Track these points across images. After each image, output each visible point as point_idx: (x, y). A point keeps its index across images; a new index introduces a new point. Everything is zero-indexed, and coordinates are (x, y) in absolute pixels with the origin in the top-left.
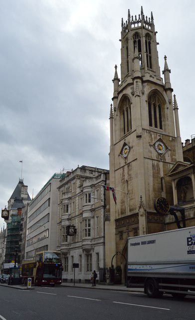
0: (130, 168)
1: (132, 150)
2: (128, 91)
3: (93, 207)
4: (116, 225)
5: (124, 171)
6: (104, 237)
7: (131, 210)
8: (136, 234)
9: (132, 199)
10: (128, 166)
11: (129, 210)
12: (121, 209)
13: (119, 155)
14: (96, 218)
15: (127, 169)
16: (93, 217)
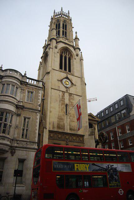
0: (71, 97)
1: (74, 86)
2: (72, 49)
5: (64, 94)
7: (71, 129)
9: (74, 122)
11: (68, 127)
13: (58, 80)
15: (68, 96)
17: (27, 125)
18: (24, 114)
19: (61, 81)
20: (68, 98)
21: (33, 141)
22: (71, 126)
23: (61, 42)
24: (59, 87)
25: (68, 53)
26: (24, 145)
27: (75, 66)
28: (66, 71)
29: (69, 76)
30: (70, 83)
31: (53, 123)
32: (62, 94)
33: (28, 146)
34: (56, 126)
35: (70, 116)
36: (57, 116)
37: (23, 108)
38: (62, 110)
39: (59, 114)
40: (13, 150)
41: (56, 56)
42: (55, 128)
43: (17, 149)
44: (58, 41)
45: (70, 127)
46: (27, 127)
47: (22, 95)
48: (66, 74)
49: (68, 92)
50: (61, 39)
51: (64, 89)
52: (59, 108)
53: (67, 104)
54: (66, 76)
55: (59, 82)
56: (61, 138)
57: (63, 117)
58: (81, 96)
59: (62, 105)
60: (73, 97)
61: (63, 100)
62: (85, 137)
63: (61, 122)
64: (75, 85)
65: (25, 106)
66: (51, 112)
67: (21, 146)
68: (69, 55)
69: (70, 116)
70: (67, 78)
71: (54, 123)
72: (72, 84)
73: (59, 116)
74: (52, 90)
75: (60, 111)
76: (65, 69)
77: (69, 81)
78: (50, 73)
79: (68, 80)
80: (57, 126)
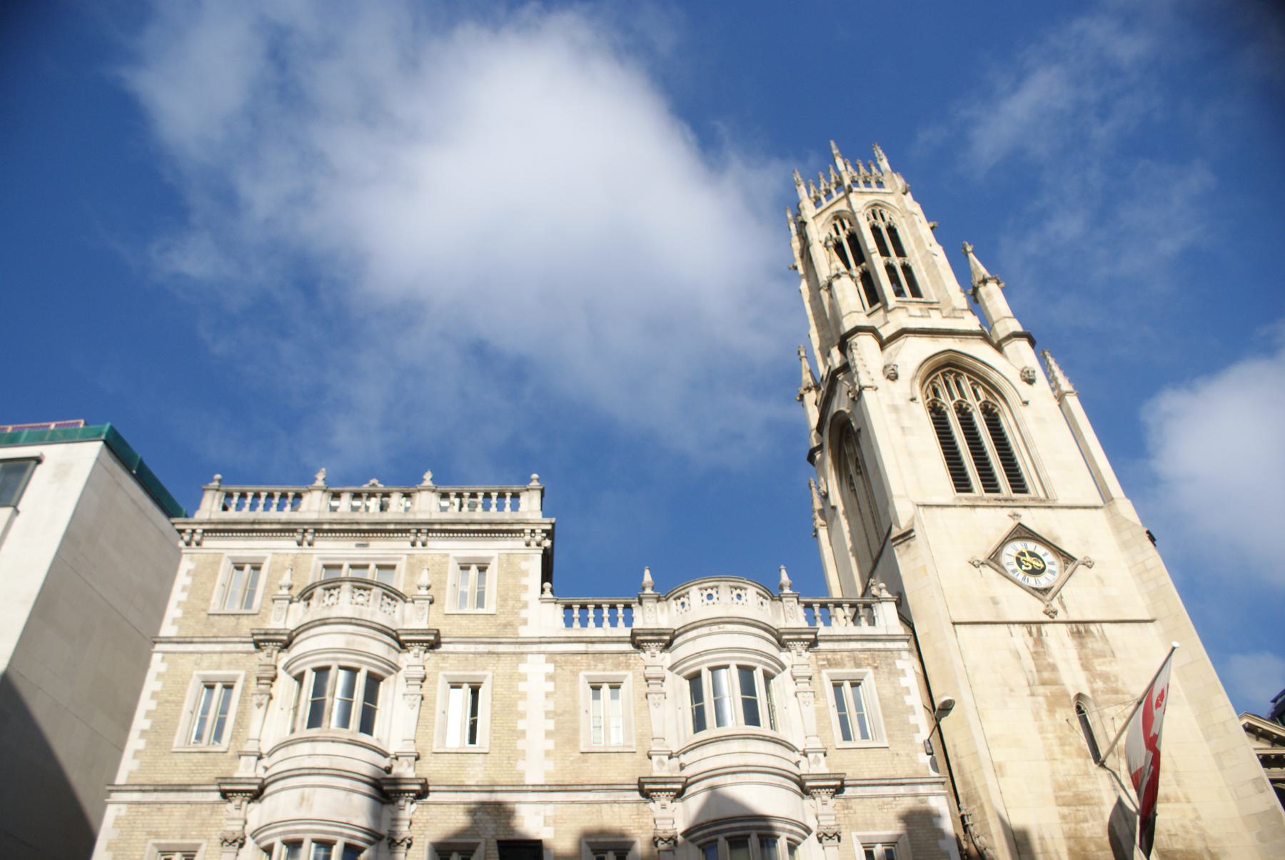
0: (1092, 644)
5: (1039, 641)
10: (1078, 635)
13: (976, 564)
19: (994, 559)
23: (904, 332)
24: (995, 602)
25: (966, 384)
27: (1040, 449)
28: (998, 491)
29: (1032, 519)
30: (1048, 557)
32: (1030, 641)
36: (1049, 790)
38: (1063, 742)
39: (1053, 773)
41: (906, 423)
44: (886, 333)
47: (810, 711)
48: (1009, 511)
49: (1061, 616)
50: (899, 320)
51: (1033, 609)
52: (1042, 730)
53: (1079, 696)
54: (1011, 524)
55: (987, 571)
57: (1085, 786)
58: (1152, 621)
59: (1051, 711)
61: (1046, 675)
63: (1085, 820)
64: (1088, 564)
65: (850, 774)
66: (998, 770)
68: (980, 391)
70: (1022, 533)
71: (1047, 836)
72: (1068, 558)
73: (1058, 787)
74: (957, 626)
75: (1056, 749)
76: (990, 484)
77: (1040, 550)
78: (917, 532)
79: (1031, 546)
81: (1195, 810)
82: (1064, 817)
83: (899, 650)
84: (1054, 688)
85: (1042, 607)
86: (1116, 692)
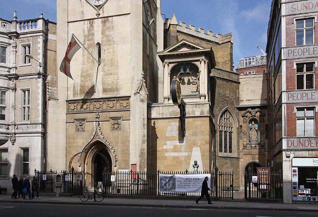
0: (108, 24)
3: (13, 72)
4: (68, 109)
5: (92, 25)
6: (44, 125)
7: (105, 90)
8: (116, 126)
10: (104, 23)
12: (81, 86)
14: (19, 92)
15: (101, 25)
16: (15, 89)
17: (29, 100)
18: (21, 84)
20: (100, 29)
21: (36, 122)
22: (105, 84)
24: (82, 13)
26: (24, 129)
31: (74, 87)
32: (89, 25)
33: (30, 130)
34: (79, 89)
35: (104, 66)
37: (17, 77)
40: (13, 138)
42: (77, 94)
43: (17, 135)
45: (103, 87)
46: (29, 104)
51: (91, 13)
56: (75, 110)
60: (112, 22)
62: (131, 99)
67: (21, 131)
69: (104, 66)
71: (76, 85)
73: (82, 72)
75: (86, 61)
80: (81, 90)
81: (118, 77)
82: (82, 81)
83: (40, 35)
84: (91, 42)
85: (96, 12)
86: (109, 41)
